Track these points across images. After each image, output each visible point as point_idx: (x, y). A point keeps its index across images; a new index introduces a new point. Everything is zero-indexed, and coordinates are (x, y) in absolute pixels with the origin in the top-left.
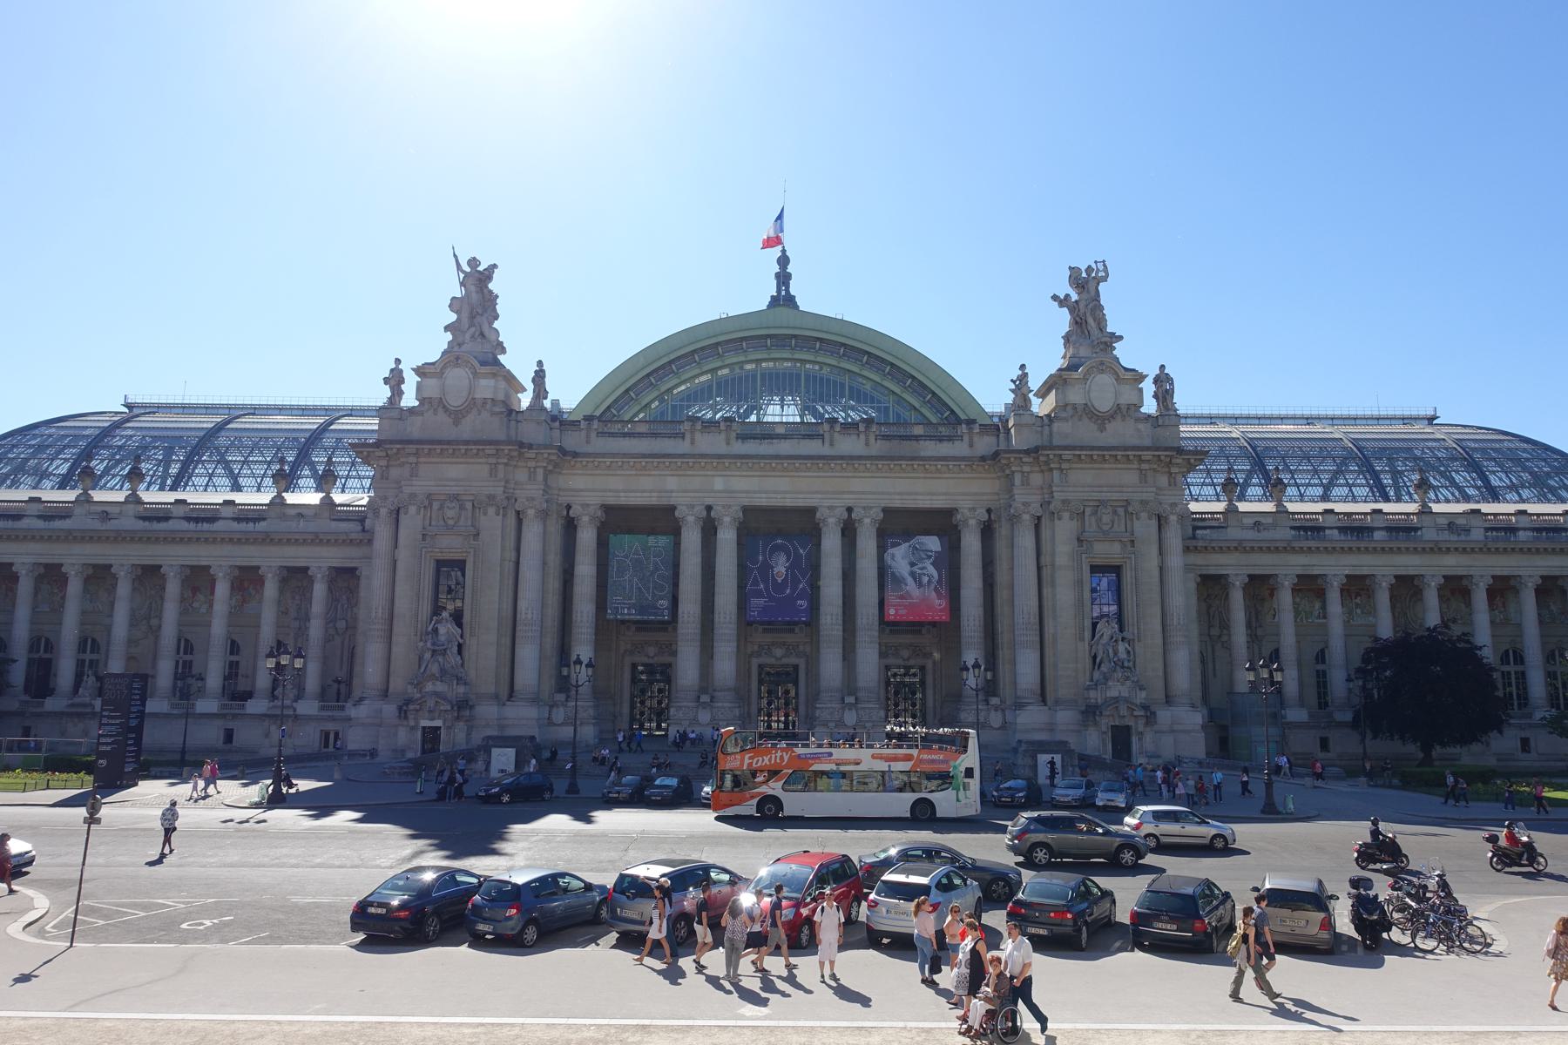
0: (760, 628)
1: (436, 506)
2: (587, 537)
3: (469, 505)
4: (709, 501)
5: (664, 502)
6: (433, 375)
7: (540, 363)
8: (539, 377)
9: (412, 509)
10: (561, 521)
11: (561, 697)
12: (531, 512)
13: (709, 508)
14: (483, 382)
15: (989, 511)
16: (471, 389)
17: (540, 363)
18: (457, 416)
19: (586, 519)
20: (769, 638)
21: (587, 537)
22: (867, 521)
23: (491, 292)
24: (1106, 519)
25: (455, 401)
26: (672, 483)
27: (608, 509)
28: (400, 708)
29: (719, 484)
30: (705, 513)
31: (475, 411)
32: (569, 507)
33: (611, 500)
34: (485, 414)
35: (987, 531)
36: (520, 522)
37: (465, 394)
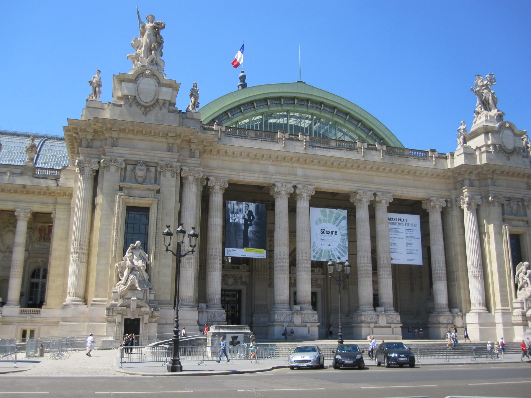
1: (129, 167)
2: (217, 199)
3: (153, 169)
6: (129, 81)
9: (113, 169)
10: (202, 189)
11: (203, 305)
12: (191, 178)
13: (295, 187)
14: (164, 89)
16: (157, 93)
18: (147, 109)
19: (217, 188)
21: (217, 199)
23: (161, 37)
24: (515, 207)
25: (146, 99)
28: (108, 309)
31: (157, 108)
32: (208, 179)
34: (165, 111)
35: (444, 213)
36: (182, 185)
37: (152, 95)
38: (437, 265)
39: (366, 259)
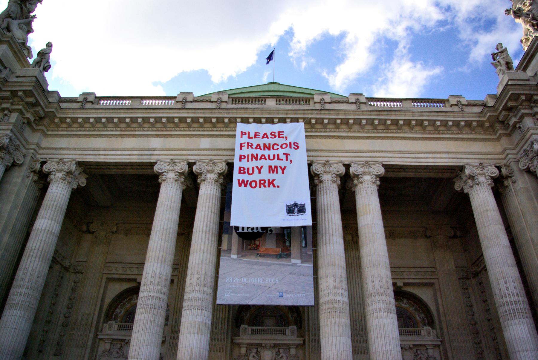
0: (250, 328)
4: (192, 159)
5: (145, 159)
7: (49, 45)
8: (44, 55)
15: (499, 168)
17: (49, 45)
20: (257, 339)
22: (367, 178)
26: (156, 143)
27: (85, 167)
29: (205, 143)
30: (186, 168)
32: (43, 163)
33: (90, 158)
35: (499, 187)
38: (503, 286)
39: (331, 279)
